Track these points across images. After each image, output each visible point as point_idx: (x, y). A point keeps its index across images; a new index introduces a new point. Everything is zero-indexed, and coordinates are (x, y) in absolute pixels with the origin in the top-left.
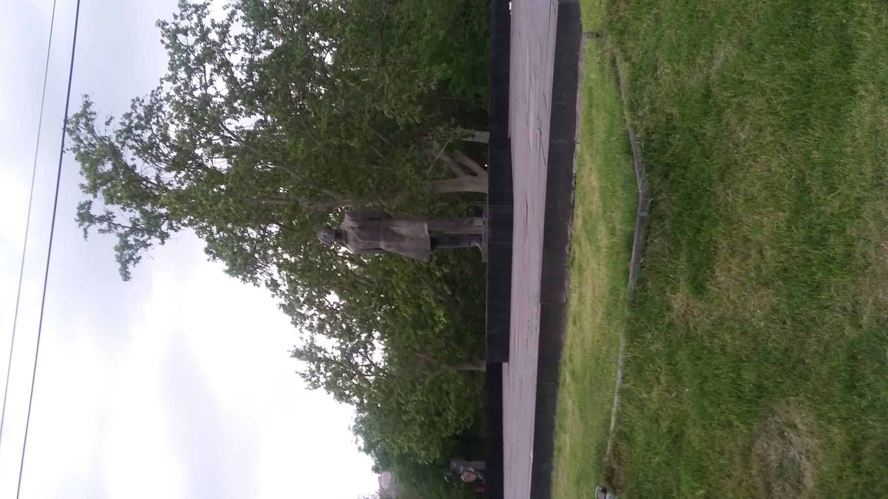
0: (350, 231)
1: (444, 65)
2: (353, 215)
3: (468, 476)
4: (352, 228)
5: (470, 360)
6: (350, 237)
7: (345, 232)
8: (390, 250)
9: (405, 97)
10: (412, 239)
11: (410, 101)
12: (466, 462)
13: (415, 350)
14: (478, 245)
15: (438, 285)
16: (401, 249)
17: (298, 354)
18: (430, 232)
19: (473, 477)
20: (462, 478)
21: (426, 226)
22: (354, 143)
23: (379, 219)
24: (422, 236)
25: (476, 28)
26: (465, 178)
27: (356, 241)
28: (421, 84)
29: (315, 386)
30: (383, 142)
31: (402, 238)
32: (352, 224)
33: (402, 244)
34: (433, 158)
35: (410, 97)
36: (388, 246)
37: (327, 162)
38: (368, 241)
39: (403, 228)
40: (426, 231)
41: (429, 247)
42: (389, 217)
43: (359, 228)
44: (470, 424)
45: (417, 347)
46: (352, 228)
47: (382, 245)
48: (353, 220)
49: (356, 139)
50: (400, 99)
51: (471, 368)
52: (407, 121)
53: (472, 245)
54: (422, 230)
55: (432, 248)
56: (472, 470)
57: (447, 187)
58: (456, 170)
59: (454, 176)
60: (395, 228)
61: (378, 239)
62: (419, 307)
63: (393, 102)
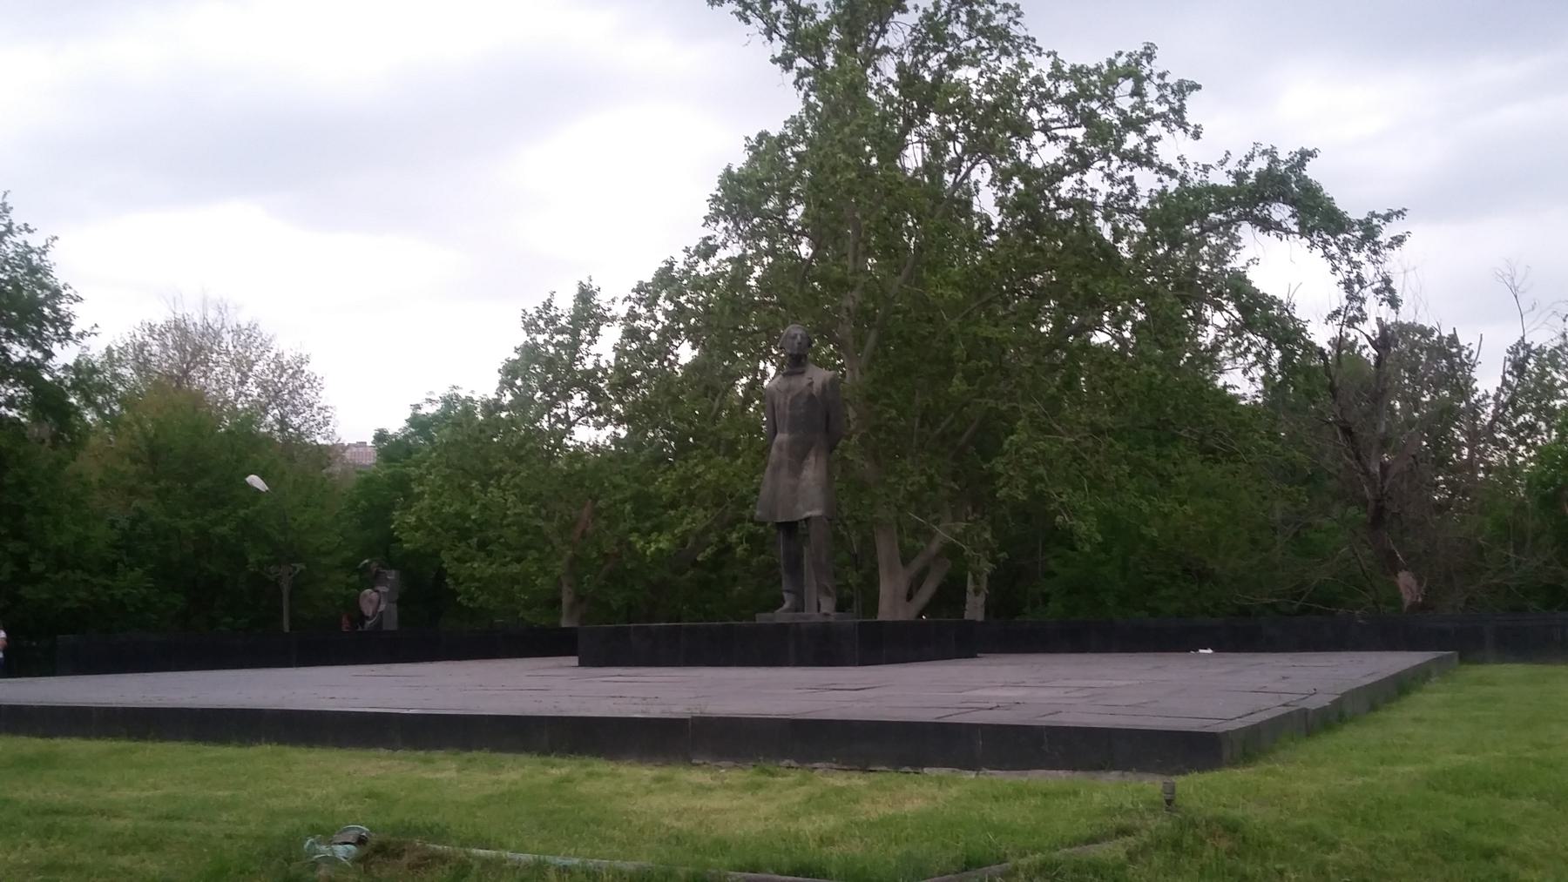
0: (804, 381)
1: (1100, 538)
2: (834, 383)
3: (371, 601)
4: (811, 384)
5: (580, 598)
6: (794, 381)
7: (802, 373)
8: (774, 451)
9: (1041, 470)
11: (1032, 481)
12: (396, 597)
13: (596, 500)
14: (786, 606)
15: (713, 537)
16: (776, 469)
17: (585, 296)
18: (807, 520)
19: (368, 609)
20: (368, 591)
21: (817, 512)
22: (958, 384)
24: (800, 506)
25: (1163, 592)
26: (902, 580)
27: (788, 390)
28: (1065, 498)
29: (530, 326)
30: (961, 434)
31: (796, 471)
32: (818, 383)
33: (784, 471)
34: (937, 522)
35: (1041, 479)
36: (780, 448)
37: (924, 338)
39: (812, 472)
40: (809, 514)
41: (780, 519)
42: (831, 448)
43: (811, 397)
44: (465, 602)
45: (601, 503)
46: (811, 384)
47: (782, 437)
48: (824, 386)
49: (965, 387)
50: (1037, 463)
51: (567, 599)
52: (1000, 475)
53: (785, 595)
54: (811, 508)
55: (779, 525)
56: (382, 607)
57: (886, 549)
58: (917, 564)
59: (905, 561)
60: (812, 459)
61: (792, 430)
62: (674, 505)
63: (1031, 451)
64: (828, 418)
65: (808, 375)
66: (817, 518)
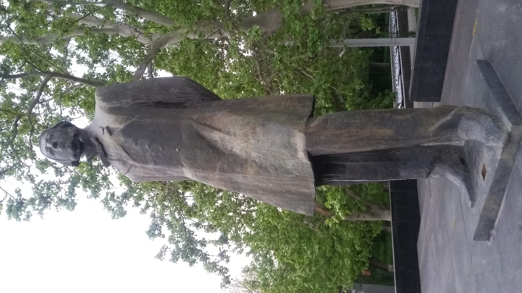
0: (106, 139)
4: (110, 131)
7: (97, 139)
10: (262, 169)
18: (311, 157)
21: (299, 141)
23: (179, 105)
24: (290, 164)
27: (124, 163)
31: (231, 162)
33: (239, 178)
38: (151, 166)
39: (235, 137)
40: (302, 155)
41: (311, 189)
43: (126, 132)
48: (111, 111)
51: (369, 218)
54: (292, 149)
60: (216, 136)
64: (159, 104)
65: (99, 132)
66: (310, 140)
